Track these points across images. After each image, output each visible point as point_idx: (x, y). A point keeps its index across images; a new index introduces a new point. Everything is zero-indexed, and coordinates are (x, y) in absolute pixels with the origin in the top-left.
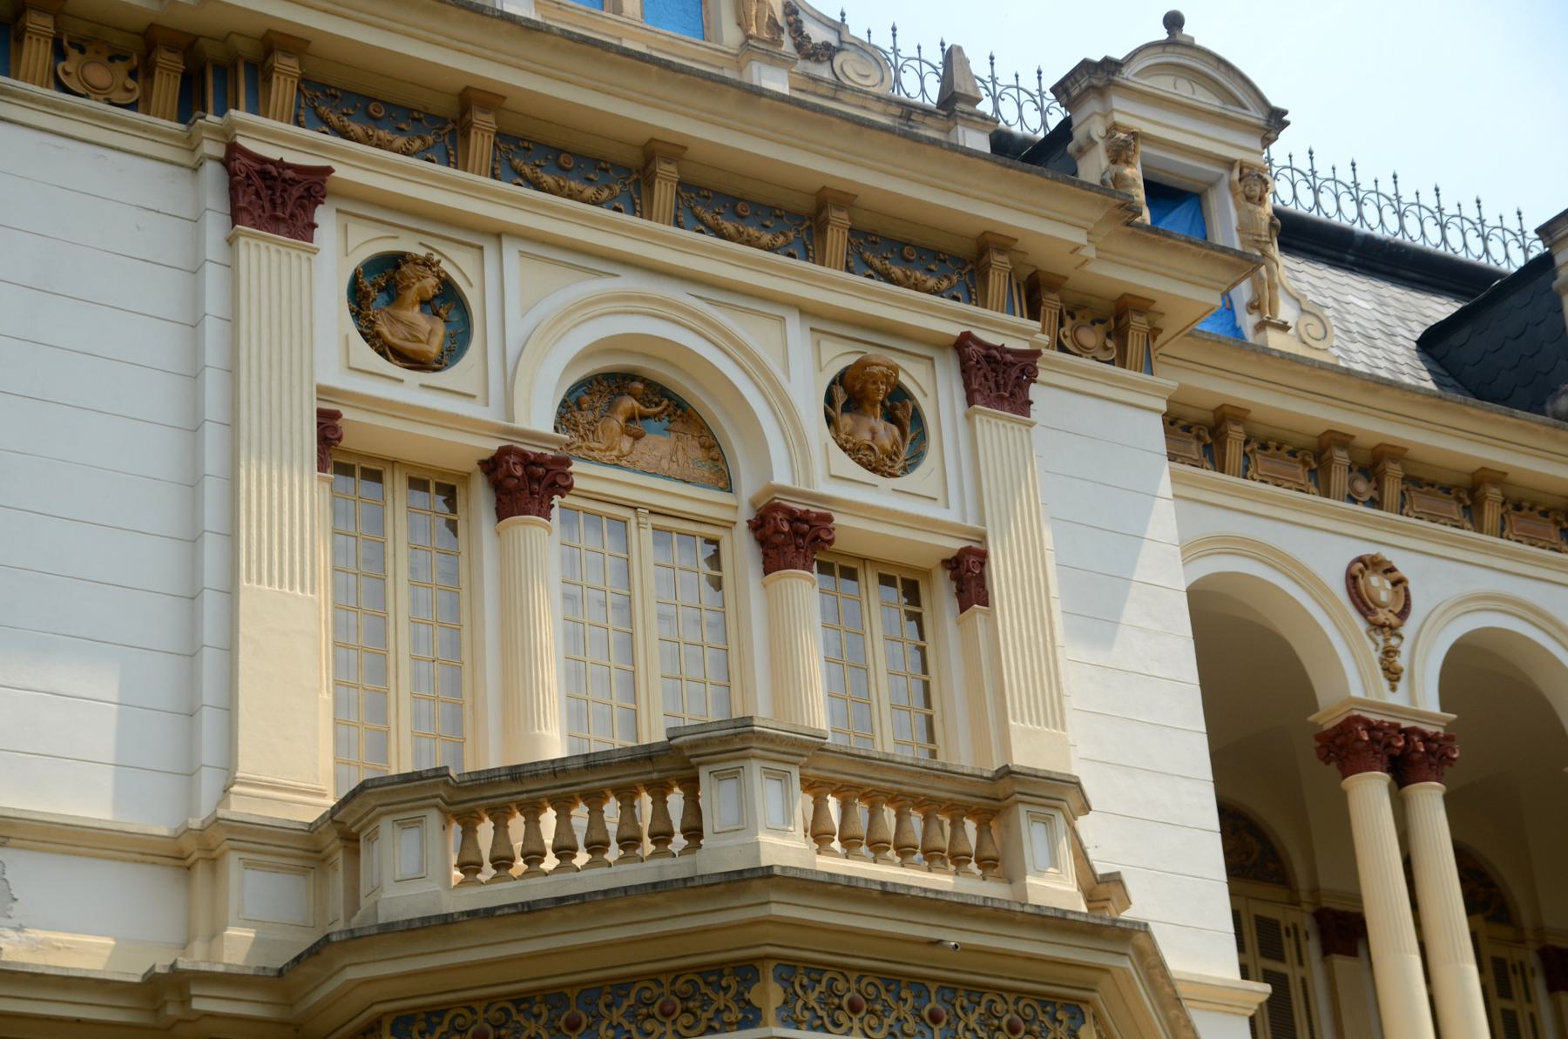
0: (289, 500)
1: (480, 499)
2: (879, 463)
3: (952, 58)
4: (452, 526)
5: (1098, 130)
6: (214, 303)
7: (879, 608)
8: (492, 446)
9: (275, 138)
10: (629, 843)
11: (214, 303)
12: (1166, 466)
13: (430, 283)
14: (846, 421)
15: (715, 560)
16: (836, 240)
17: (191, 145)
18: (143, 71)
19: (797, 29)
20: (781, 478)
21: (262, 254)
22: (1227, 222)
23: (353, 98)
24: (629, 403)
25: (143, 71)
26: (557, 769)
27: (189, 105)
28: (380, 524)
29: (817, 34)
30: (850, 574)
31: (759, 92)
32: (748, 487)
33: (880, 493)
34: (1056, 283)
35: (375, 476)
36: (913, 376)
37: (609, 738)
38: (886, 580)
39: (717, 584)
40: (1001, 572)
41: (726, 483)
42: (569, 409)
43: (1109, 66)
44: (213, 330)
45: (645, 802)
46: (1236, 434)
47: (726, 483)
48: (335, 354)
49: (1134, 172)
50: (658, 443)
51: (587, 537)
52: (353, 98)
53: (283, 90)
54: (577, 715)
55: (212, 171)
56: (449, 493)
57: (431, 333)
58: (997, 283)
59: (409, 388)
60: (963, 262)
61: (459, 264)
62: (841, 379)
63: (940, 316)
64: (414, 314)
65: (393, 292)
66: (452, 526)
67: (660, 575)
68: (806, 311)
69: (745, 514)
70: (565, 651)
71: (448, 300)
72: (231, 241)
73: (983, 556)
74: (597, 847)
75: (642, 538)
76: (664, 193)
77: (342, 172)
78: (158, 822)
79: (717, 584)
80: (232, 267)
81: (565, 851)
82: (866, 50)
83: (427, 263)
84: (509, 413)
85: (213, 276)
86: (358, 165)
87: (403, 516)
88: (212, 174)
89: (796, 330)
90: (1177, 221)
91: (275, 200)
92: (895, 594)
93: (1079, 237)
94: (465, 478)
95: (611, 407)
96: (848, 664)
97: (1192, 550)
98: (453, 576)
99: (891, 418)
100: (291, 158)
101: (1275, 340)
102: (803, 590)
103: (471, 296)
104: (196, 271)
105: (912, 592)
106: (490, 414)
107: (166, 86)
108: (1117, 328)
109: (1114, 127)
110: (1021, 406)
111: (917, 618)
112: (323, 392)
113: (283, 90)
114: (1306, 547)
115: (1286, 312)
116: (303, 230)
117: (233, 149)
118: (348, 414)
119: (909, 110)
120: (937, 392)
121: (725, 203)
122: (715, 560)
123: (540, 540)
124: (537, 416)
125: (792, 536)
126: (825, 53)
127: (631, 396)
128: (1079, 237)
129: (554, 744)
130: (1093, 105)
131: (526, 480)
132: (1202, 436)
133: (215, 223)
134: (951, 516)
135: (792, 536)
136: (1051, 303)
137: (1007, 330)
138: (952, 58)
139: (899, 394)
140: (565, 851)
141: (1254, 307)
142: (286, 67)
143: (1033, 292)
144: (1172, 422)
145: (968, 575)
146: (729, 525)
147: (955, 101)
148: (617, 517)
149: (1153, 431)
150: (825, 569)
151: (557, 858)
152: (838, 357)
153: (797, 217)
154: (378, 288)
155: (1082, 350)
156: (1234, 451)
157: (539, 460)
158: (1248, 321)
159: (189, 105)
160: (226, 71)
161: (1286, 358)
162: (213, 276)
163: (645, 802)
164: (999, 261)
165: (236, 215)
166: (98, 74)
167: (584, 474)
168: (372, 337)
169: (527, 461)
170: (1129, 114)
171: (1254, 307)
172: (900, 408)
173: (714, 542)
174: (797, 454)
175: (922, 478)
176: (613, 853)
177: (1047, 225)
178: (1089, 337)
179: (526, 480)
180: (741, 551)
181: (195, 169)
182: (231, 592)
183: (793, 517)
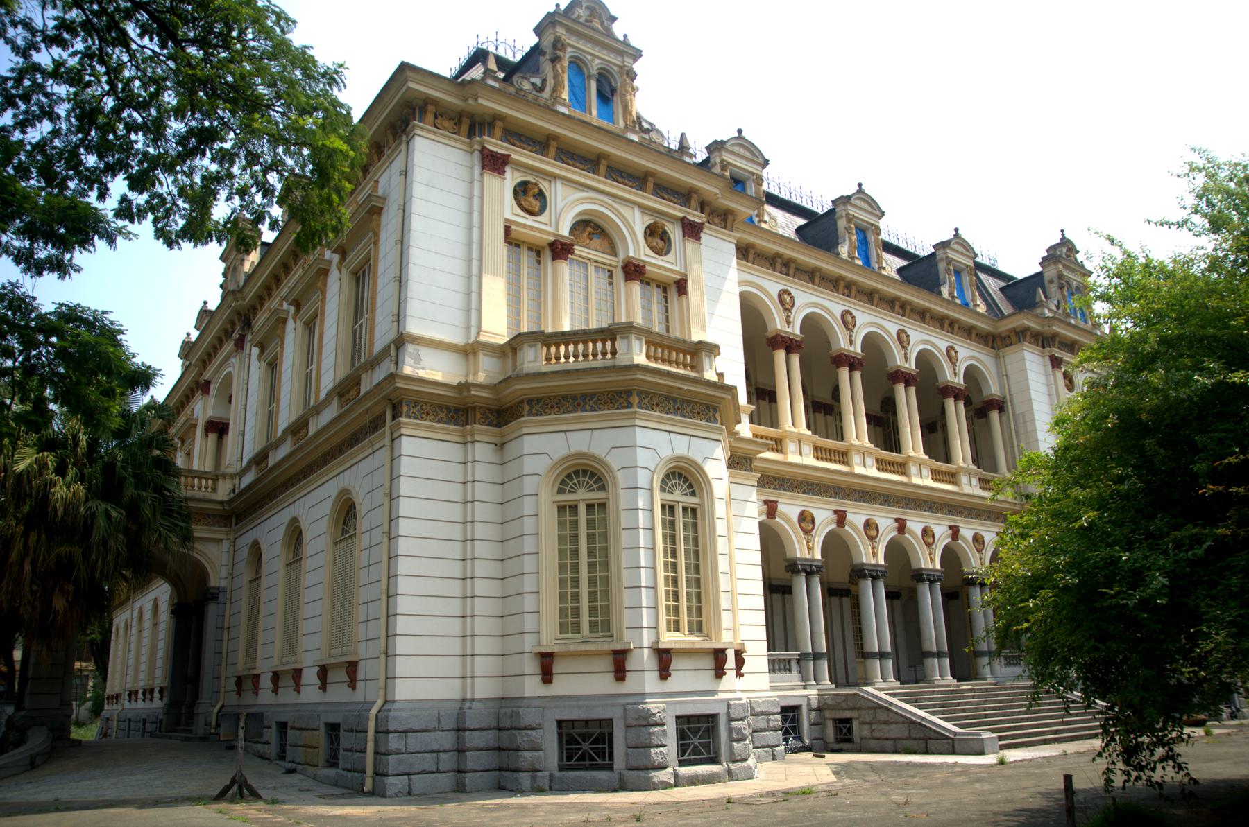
0: (497, 249)
1: (547, 254)
2: (659, 252)
3: (683, 136)
4: (539, 262)
5: (718, 161)
6: (476, 192)
7: (656, 294)
8: (552, 239)
9: (496, 145)
10: (585, 356)
11: (476, 192)
12: (735, 260)
13: (536, 190)
14: (649, 239)
15: (611, 276)
16: (650, 186)
17: (471, 146)
18: (459, 124)
19: (640, 123)
20: (632, 254)
21: (490, 179)
22: (751, 189)
23: (517, 135)
24: (589, 229)
25: (459, 124)
26: (563, 334)
27: (471, 134)
28: (519, 260)
29: (646, 126)
30: (648, 284)
31: (632, 141)
32: (622, 256)
33: (658, 261)
34: (709, 204)
35: (518, 246)
36: (669, 228)
37: (580, 326)
38: (658, 286)
39: (611, 284)
40: (691, 286)
41: (615, 254)
42: (573, 229)
43: (722, 142)
44: (476, 200)
45: (591, 345)
46: (752, 251)
47: (615, 254)
48: (509, 209)
49: (727, 174)
50: (597, 242)
51: (576, 268)
52: (517, 135)
53: (498, 131)
54: (572, 319)
55: (477, 153)
56: (538, 253)
57: (536, 205)
58: (693, 203)
59: (529, 221)
60: (684, 195)
61: (544, 185)
62: (649, 227)
63: (677, 211)
64: (531, 199)
65: (525, 192)
66: (539, 262)
67: (596, 281)
68: (641, 206)
69: (620, 264)
70: (574, 300)
71: (541, 196)
72: (482, 175)
73: (686, 281)
74: (576, 357)
75: (591, 269)
76: (603, 169)
77: (513, 156)
78: (456, 338)
79: (611, 284)
80: (482, 182)
81: (567, 357)
82: (658, 131)
83: (536, 184)
84: (557, 229)
85: (476, 184)
86: (520, 155)
87: (526, 258)
88: (477, 154)
89: (637, 212)
90: (739, 188)
91: (494, 163)
92: (660, 290)
93: (717, 191)
94: (543, 248)
95: (584, 230)
96: (647, 309)
97: (741, 283)
98: (539, 276)
99: (662, 239)
100: (500, 151)
101: (763, 225)
102: (636, 287)
103: (547, 195)
104: (471, 183)
105: (665, 290)
106: (552, 230)
107: (465, 128)
108: (724, 218)
109: (722, 161)
110: (699, 239)
111: (666, 298)
112: (507, 220)
113: (498, 131)
114: (770, 285)
115: (766, 218)
116: (502, 173)
117: (484, 148)
118: (513, 227)
119: (670, 150)
120: (675, 233)
121: (620, 173)
122: (611, 276)
123: (564, 267)
124: (565, 231)
125: (634, 271)
126: (647, 131)
127: (589, 227)
128: (717, 191)
129: (566, 327)
130: (717, 153)
131: (560, 250)
132: (745, 252)
133: (477, 170)
134: (678, 269)
135: (634, 271)
136: (707, 209)
137: (696, 216)
138: (683, 136)
139: (665, 232)
140: (567, 357)
141: (758, 216)
142: (499, 124)
143: (703, 206)
144: (738, 248)
145: (681, 286)
146: (616, 267)
147: (683, 147)
148: (584, 263)
149: (732, 249)
150: (642, 282)
151: (567, 357)
152: (649, 220)
153: (639, 179)
154: (521, 191)
155: (714, 224)
156: (751, 256)
157: (565, 244)
158: (756, 220)
159: (471, 134)
160: (481, 125)
161: (767, 230)
162: (476, 184)
163: (591, 345)
164: (694, 196)
165: (483, 167)
166: (446, 124)
167: (578, 250)
168: (520, 205)
169: (562, 244)
170: (727, 157)
171: (758, 216)
172: (664, 237)
173: (611, 272)
174: (638, 249)
175: (669, 257)
176: (581, 359)
177: (710, 188)
178: (717, 220)
179: (560, 250)
180: (619, 275)
181: (472, 153)
182: (480, 277)
183: (635, 266)
